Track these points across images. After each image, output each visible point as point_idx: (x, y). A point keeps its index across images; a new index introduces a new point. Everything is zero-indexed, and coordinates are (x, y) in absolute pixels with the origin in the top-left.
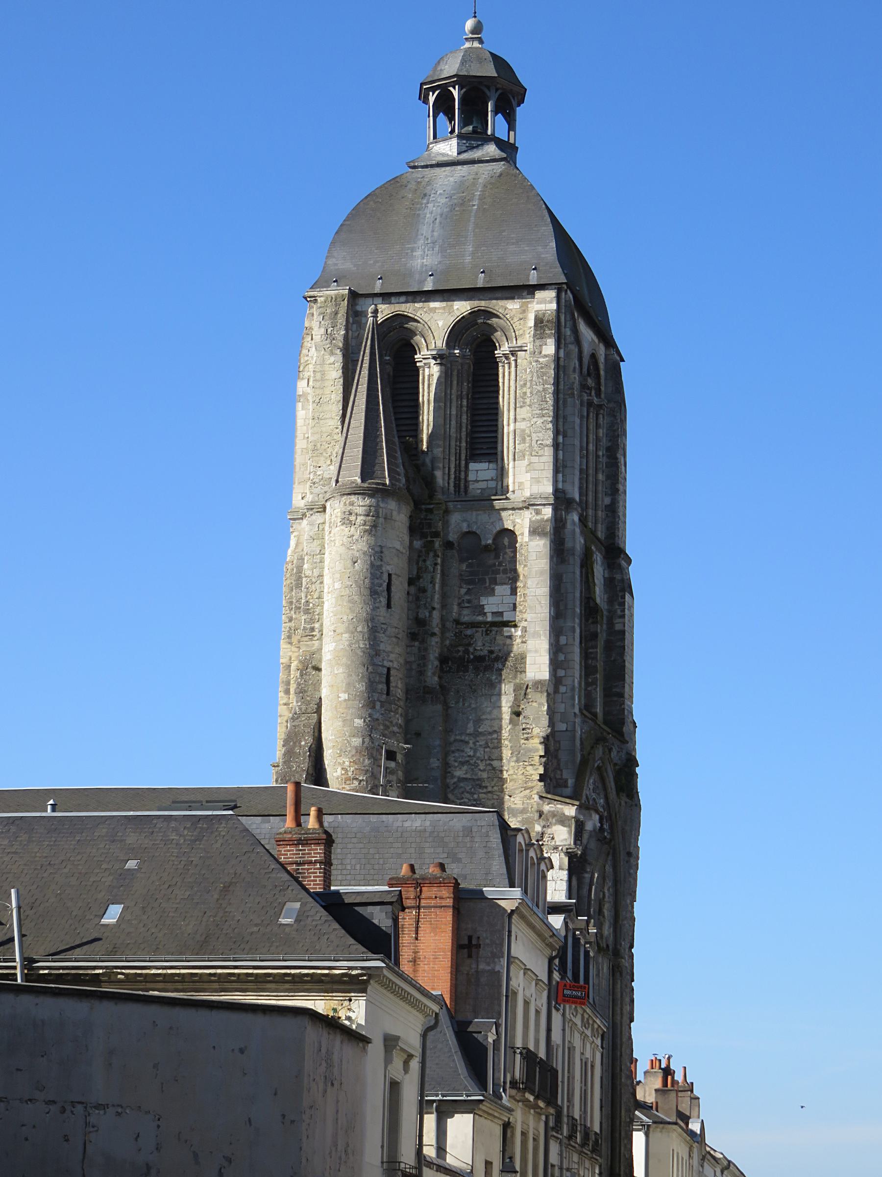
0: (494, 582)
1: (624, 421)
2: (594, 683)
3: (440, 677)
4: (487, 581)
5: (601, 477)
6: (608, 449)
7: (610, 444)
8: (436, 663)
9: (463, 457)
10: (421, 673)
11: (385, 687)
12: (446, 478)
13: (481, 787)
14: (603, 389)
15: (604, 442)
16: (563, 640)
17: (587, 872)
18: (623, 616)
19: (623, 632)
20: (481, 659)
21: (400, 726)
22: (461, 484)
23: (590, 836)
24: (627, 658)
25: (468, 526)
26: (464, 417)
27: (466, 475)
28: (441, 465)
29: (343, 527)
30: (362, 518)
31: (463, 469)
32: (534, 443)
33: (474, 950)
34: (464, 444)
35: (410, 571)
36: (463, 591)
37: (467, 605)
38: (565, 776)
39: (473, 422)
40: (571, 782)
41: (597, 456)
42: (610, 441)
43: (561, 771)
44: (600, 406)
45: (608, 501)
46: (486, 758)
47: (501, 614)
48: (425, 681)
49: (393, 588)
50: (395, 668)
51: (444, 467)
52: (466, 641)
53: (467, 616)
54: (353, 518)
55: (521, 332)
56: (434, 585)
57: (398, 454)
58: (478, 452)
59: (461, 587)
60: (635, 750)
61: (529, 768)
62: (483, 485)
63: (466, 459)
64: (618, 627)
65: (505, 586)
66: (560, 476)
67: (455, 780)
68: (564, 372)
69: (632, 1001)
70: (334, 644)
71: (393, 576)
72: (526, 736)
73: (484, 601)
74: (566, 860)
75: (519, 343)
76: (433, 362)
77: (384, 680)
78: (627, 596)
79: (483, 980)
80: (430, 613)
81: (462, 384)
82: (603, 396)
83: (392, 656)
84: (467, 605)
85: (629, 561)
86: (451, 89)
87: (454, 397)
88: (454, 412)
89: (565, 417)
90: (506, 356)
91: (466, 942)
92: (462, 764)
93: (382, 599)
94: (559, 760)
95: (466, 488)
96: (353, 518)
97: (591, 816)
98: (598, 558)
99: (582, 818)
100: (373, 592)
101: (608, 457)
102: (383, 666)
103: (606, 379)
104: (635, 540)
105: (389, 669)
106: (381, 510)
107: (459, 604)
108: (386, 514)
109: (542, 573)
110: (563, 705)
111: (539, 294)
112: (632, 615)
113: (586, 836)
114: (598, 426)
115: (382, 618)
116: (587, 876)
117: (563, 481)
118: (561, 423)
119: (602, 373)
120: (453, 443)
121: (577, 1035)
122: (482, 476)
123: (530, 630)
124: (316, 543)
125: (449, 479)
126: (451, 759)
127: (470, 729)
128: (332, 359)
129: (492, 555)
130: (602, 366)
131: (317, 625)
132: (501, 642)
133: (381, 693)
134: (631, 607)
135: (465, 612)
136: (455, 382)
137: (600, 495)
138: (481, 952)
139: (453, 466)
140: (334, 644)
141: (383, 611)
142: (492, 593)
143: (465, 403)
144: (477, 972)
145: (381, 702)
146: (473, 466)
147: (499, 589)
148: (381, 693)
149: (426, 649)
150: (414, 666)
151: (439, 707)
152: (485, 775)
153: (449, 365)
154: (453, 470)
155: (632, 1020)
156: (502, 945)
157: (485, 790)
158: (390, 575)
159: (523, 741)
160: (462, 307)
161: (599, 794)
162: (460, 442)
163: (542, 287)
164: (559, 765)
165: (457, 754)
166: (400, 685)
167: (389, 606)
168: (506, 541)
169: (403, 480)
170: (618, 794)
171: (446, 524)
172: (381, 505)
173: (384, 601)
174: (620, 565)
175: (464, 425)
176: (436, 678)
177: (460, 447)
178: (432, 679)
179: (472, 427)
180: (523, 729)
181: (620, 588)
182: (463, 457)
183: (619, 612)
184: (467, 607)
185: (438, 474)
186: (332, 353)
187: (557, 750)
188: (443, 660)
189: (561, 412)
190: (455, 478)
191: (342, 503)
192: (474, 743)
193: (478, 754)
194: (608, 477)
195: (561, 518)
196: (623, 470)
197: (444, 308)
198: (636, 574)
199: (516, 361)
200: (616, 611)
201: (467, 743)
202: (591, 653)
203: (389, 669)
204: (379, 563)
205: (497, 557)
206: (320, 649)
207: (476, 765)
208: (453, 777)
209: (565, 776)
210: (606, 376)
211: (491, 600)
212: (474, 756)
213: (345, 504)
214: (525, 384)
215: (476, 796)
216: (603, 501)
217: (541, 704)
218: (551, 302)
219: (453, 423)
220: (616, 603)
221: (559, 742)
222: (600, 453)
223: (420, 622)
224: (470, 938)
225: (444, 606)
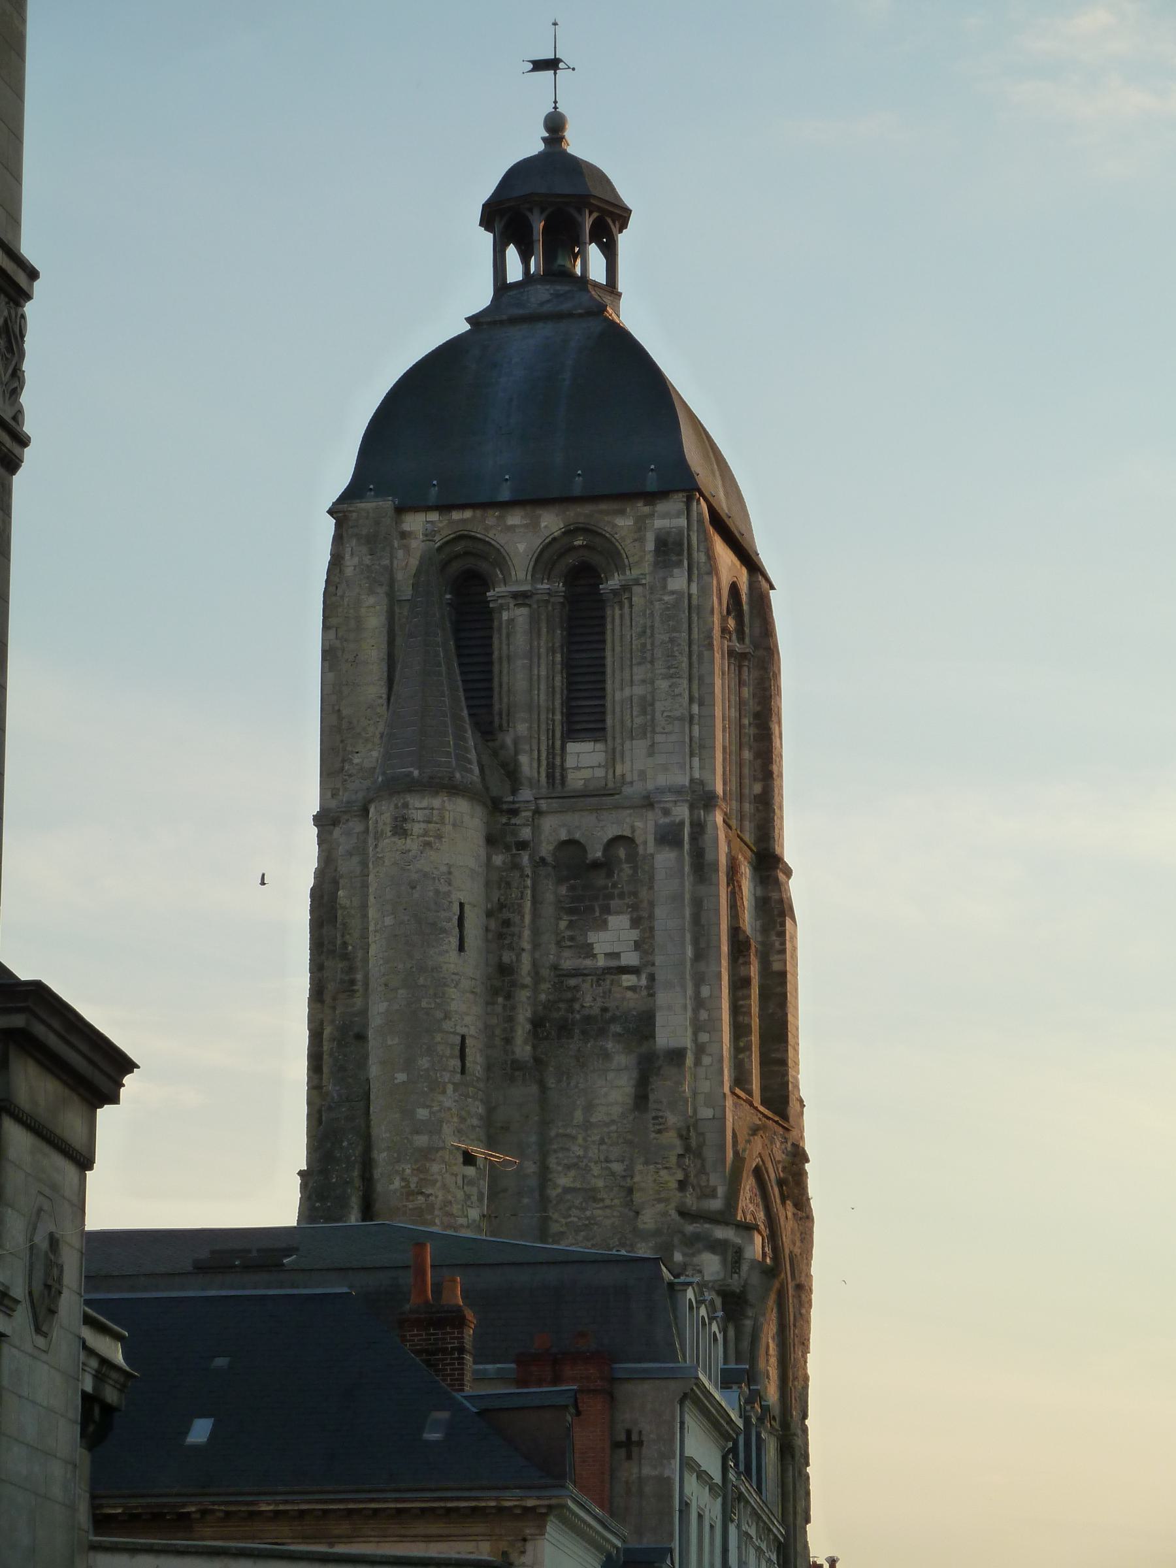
0: (607, 910)
1: (777, 675)
3: (534, 1047)
4: (597, 909)
5: (747, 755)
6: (757, 715)
7: (758, 708)
8: (528, 1027)
10: (508, 1041)
11: (459, 1063)
12: (535, 765)
13: (595, 1200)
14: (747, 630)
16: (705, 991)
17: (747, 1317)
18: (783, 951)
19: (783, 975)
20: (588, 1019)
21: (481, 1118)
22: (556, 774)
24: (790, 1010)
25: (569, 832)
26: (558, 678)
27: (563, 760)
28: (527, 747)
29: (393, 839)
30: (423, 826)
31: (558, 751)
32: (658, 715)
33: (635, 1450)
34: (558, 717)
35: (488, 899)
36: (563, 924)
38: (712, 1183)
39: (571, 685)
40: (721, 1191)
42: (759, 704)
43: (708, 1174)
45: (758, 788)
46: (602, 1158)
47: (616, 955)
48: (513, 1053)
49: (467, 924)
50: (472, 1036)
51: (532, 750)
52: (569, 995)
53: (568, 962)
54: (407, 826)
55: (636, 558)
56: (523, 916)
57: (469, 734)
58: (578, 727)
59: (561, 919)
60: (802, 1137)
61: (663, 1173)
62: (587, 774)
64: (776, 967)
65: (621, 917)
66: (696, 760)
67: (559, 1190)
68: (698, 614)
69: (808, 1493)
70: (386, 1004)
71: (467, 908)
73: (592, 937)
75: (635, 572)
76: (511, 600)
77: (457, 1052)
78: (788, 921)
79: (648, 1489)
80: (518, 956)
82: (747, 640)
83: (468, 1020)
85: (788, 873)
86: (528, 214)
87: (543, 650)
88: (543, 673)
89: (701, 678)
90: (615, 592)
91: (622, 1437)
92: (568, 1167)
93: (451, 939)
94: (703, 1160)
95: (563, 778)
96: (407, 826)
98: (746, 870)
102: (455, 1033)
104: (795, 842)
105: (463, 1037)
106: (447, 814)
107: (558, 943)
110: (708, 1083)
111: (662, 507)
112: (795, 949)
113: (745, 1267)
114: (741, 683)
115: (452, 966)
116: (748, 1323)
117: (701, 768)
118: (695, 686)
119: (745, 607)
120: (543, 717)
121: (752, 1551)
122: (586, 761)
123: (660, 977)
124: (356, 859)
125: (539, 767)
126: (552, 1162)
127: (579, 1115)
128: (371, 600)
130: (744, 598)
131: (359, 976)
132: (618, 996)
133: (454, 1071)
134: (794, 937)
135: (567, 953)
136: (544, 630)
137: (746, 781)
138: (645, 1450)
139: (543, 748)
140: (386, 1004)
142: (604, 925)
143: (558, 658)
144: (640, 1478)
145: (454, 1084)
146: (572, 747)
147: (614, 921)
148: (454, 1071)
149: (513, 1008)
150: (498, 1032)
151: (534, 1089)
152: (600, 1183)
153: (535, 606)
155: (808, 1520)
156: (672, 1440)
157: (601, 1205)
158: (462, 905)
159: (653, 1135)
160: (551, 522)
161: (757, 1205)
163: (663, 494)
164: (703, 1166)
165: (560, 1155)
166: (479, 1059)
167: (461, 948)
168: (622, 853)
169: (476, 770)
170: (783, 1203)
171: (536, 829)
173: (454, 941)
175: (558, 690)
176: (528, 1048)
177: (553, 720)
178: (523, 1050)
179: (569, 691)
181: (775, 912)
182: (558, 734)
184: (570, 947)
185: (524, 759)
186: (371, 592)
187: (701, 1146)
188: (537, 1023)
189: (695, 670)
190: (548, 764)
191: (392, 806)
192: (585, 1140)
193: (590, 1154)
195: (699, 818)
196: (778, 744)
197: (526, 526)
198: (798, 889)
199: (630, 599)
201: (574, 1138)
202: (742, 1006)
203: (463, 1037)
205: (610, 875)
206: (364, 1012)
207: (588, 1169)
208: (555, 1186)
209: (712, 1183)
210: (751, 612)
212: (584, 1157)
213: (396, 807)
214: (644, 632)
215: (588, 1213)
216: (751, 789)
218: (678, 516)
219: (543, 687)
220: (773, 933)
221: (703, 1134)
222: (746, 721)
223: (505, 971)
224: (629, 1433)
225: (536, 946)
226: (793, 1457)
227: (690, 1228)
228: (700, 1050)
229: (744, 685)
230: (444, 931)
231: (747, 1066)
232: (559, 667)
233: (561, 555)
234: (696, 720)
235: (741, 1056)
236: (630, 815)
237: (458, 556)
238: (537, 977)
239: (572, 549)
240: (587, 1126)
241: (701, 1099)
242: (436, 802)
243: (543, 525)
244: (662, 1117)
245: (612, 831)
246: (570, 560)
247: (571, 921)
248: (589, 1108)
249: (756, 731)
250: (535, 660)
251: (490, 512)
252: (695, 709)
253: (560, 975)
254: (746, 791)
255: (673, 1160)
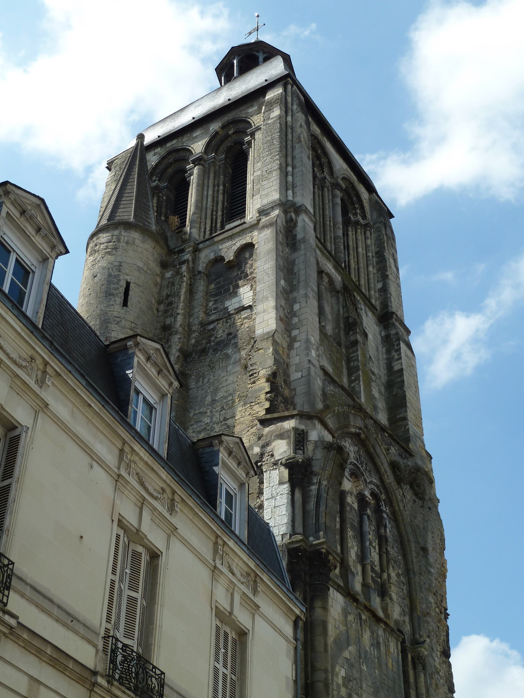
0: (237, 287)
2: (358, 379)
6: (377, 253)
7: (378, 249)
9: (219, 221)
12: (202, 234)
15: (373, 248)
16: (296, 307)
17: (313, 484)
18: (400, 358)
23: (316, 447)
25: (215, 254)
34: (220, 213)
37: (215, 311)
41: (367, 257)
44: (366, 225)
45: (380, 285)
46: (222, 419)
49: (131, 293)
51: (200, 228)
55: (258, 121)
59: (210, 301)
63: (222, 222)
65: (246, 287)
66: (290, 192)
71: (132, 286)
72: (252, 380)
73: (227, 303)
74: (286, 472)
80: (175, 318)
81: (219, 177)
84: (215, 311)
85: (408, 332)
88: (210, 192)
93: (117, 299)
97: (315, 425)
99: (302, 427)
100: (108, 294)
101: (378, 257)
103: (371, 212)
106: (123, 238)
108: (128, 240)
109: (269, 252)
110: (298, 357)
113: (310, 447)
120: (209, 212)
129: (236, 269)
141: (117, 309)
143: (221, 187)
147: (242, 290)
153: (207, 166)
154: (208, 228)
158: (128, 284)
159: (250, 386)
162: (217, 213)
165: (195, 426)
167: (125, 303)
172: (123, 233)
173: (119, 300)
174: (393, 325)
180: (250, 376)
182: (219, 221)
183: (396, 357)
184: (214, 313)
192: (211, 412)
194: (379, 270)
197: (203, 133)
200: (393, 357)
204: (117, 273)
211: (234, 300)
212: (210, 422)
216: (375, 285)
217: (266, 349)
219: (210, 199)
220: (393, 351)
221: (295, 389)
222: (370, 254)
226: (424, 668)
227: (267, 430)
228: (293, 340)
229: (368, 238)
230: (113, 295)
231: (357, 389)
232: (221, 191)
233: (222, 141)
234: (290, 173)
235: (353, 385)
236: (251, 232)
237: (171, 164)
238: (188, 329)
239: (227, 136)
240: (214, 401)
241: (292, 369)
242: (116, 232)
243: (211, 129)
244: (255, 373)
245: (238, 245)
246: (228, 143)
247: (216, 300)
248: (216, 391)
249: (377, 260)
250: (206, 188)
251: (185, 136)
252: (290, 169)
253: (203, 325)
254: (372, 285)
255: (263, 397)
